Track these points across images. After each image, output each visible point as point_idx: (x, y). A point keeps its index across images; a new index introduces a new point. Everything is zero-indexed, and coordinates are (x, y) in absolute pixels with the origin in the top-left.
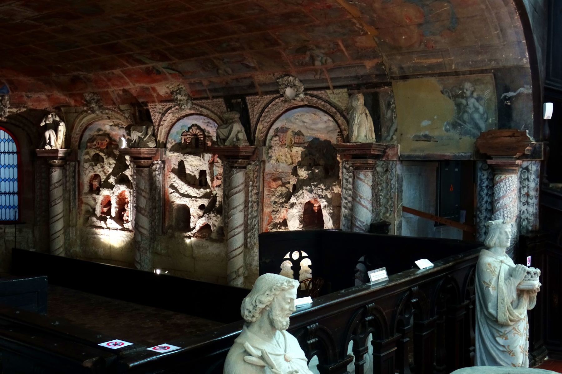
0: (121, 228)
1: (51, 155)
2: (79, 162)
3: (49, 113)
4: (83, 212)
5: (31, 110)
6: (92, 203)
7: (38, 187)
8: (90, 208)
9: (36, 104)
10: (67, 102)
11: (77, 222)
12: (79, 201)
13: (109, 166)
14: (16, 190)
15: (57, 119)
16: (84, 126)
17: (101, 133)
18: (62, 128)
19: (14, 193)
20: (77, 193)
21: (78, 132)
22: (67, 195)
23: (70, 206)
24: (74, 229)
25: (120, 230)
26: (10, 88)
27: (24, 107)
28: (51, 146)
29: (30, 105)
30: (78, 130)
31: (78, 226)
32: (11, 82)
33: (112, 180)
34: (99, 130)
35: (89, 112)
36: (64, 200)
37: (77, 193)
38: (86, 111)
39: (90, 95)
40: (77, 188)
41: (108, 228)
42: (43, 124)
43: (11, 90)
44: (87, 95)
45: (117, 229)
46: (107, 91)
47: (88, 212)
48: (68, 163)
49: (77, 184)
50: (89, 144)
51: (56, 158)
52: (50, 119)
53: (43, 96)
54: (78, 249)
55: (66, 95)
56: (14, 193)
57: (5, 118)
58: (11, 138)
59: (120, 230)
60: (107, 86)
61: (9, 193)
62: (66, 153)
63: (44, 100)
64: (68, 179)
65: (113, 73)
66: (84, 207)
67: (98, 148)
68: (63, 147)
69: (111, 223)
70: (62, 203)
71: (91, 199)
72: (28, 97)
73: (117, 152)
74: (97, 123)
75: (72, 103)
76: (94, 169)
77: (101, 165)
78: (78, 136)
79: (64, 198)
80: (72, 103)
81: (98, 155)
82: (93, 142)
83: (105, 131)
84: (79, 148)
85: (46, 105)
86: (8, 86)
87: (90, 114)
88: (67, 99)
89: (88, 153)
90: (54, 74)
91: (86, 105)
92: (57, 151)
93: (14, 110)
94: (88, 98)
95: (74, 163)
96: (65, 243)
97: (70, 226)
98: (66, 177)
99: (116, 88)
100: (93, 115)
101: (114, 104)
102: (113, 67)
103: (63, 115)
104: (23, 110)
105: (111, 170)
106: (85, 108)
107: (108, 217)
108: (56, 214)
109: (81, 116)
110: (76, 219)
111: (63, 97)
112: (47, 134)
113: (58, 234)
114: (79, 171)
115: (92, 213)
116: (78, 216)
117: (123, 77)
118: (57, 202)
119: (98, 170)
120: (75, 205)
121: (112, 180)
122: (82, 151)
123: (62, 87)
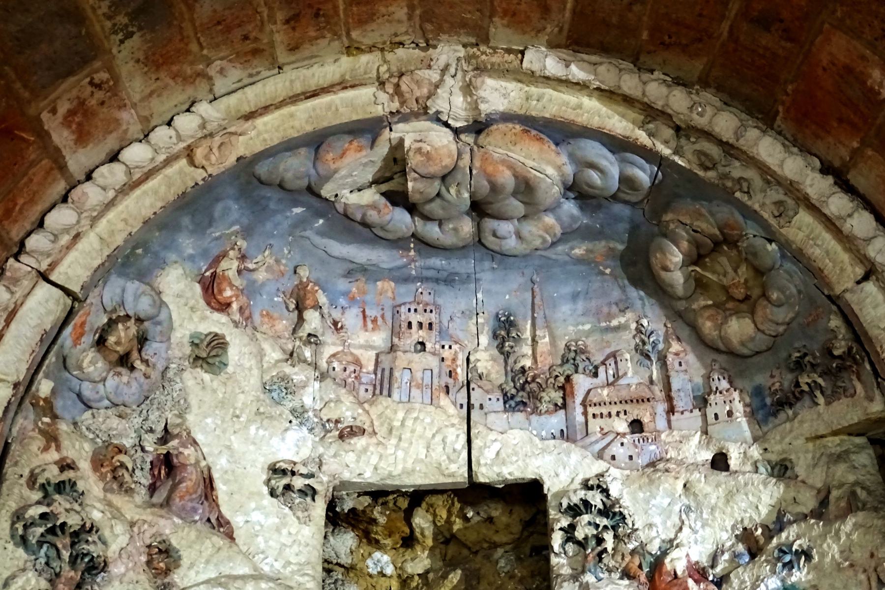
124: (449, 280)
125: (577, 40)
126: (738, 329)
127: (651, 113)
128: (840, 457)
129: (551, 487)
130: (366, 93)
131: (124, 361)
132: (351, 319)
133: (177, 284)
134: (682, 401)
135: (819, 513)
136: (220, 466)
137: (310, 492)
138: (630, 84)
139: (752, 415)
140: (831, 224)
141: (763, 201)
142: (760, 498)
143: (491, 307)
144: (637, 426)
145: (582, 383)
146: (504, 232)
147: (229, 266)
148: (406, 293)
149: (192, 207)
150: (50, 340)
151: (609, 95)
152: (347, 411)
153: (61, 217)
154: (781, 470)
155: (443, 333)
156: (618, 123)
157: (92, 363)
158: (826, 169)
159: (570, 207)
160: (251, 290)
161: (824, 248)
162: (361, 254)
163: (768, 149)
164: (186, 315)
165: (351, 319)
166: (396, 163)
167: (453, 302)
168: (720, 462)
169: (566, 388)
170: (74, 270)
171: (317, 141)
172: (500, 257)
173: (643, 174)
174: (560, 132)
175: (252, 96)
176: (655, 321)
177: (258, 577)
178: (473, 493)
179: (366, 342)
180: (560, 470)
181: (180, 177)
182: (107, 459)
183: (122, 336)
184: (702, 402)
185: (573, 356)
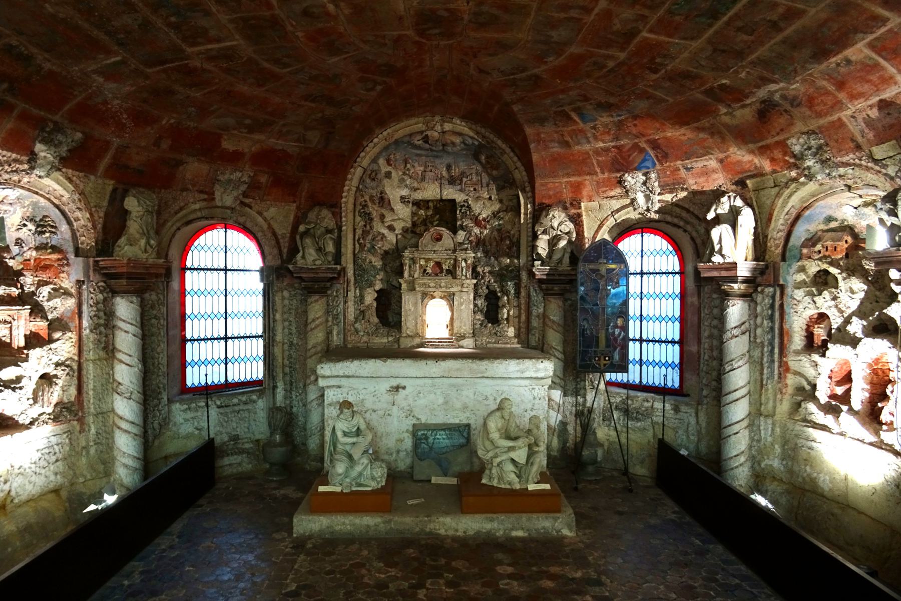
0: (873, 439)
1: (724, 274)
2: (782, 288)
3: (723, 194)
4: (790, 390)
5: (694, 193)
6: (810, 372)
7: (706, 334)
8: (805, 384)
9: (702, 180)
10: (756, 167)
11: (775, 407)
12: (780, 366)
13: (852, 292)
14: (677, 338)
15: (739, 202)
16: (794, 213)
17: (833, 225)
18: (747, 219)
19: (673, 342)
20: (776, 350)
21: (781, 227)
22: (757, 353)
23: (762, 374)
24: (770, 421)
25: (871, 444)
26: (657, 156)
27: (683, 189)
28: (723, 256)
29: (693, 183)
30: (781, 221)
31: (777, 417)
32: (655, 145)
33: (856, 327)
34: (830, 219)
35: (802, 179)
36: (751, 361)
37: (776, 350)
38: (795, 180)
39: (801, 140)
40: (777, 341)
41: (842, 434)
42: (711, 216)
43: (659, 161)
44: (794, 141)
45: (862, 441)
46: (840, 119)
47: (800, 390)
48: (759, 289)
49: (777, 331)
50: (805, 251)
51: (734, 279)
52: (724, 207)
53: (713, 163)
54: (776, 463)
55: (751, 152)
56: (673, 342)
57: (656, 212)
58: (671, 248)
59: (871, 444)
60: (838, 105)
61: (667, 342)
62: (754, 270)
63: (714, 171)
64: (759, 320)
65: (848, 62)
66: (791, 380)
67: (825, 257)
68: (750, 257)
69: (848, 423)
70: (746, 368)
71: (807, 365)
72: (687, 169)
73: (870, 266)
74: (822, 203)
75: (767, 166)
76: (815, 302)
77: (830, 293)
78: (782, 235)
79: (750, 357)
80: (767, 166)
81: (826, 272)
82: (814, 245)
83: (844, 221)
84: (784, 259)
85: (719, 180)
86: (651, 153)
87: (804, 184)
88: (756, 161)
89: (802, 269)
90: (723, 110)
91: (795, 166)
92: (733, 266)
93: (668, 197)
94: (797, 149)
95: (771, 289)
96: (750, 447)
97: (761, 415)
98: (756, 317)
99: (860, 104)
100: (812, 187)
101: (858, 147)
102: (843, 41)
103: (752, 194)
104: (682, 195)
105: (854, 305)
106: (793, 174)
107: (845, 408)
108: (733, 388)
109: (787, 192)
110: (775, 401)
111: (747, 158)
112: (715, 233)
113: (736, 428)
114: (782, 306)
115: (808, 392)
116: (779, 396)
117: (876, 66)
118: (736, 366)
119: (824, 303)
120: (772, 372)
121: (856, 327)
122: (790, 265)
123: (743, 136)
124: (437, 157)
125: (463, 118)
126: (495, 173)
127: (477, 133)
128: (511, 200)
129: (458, 201)
130: (421, 125)
131: (373, 179)
132: (416, 164)
133: (382, 161)
134: (484, 185)
135: (505, 211)
136: (391, 197)
137: (409, 202)
138: (474, 127)
139: (497, 190)
140: (511, 158)
141: (498, 152)
142: (497, 207)
143: (446, 162)
144: (475, 190)
145: (465, 180)
146: (449, 149)
147: (392, 156)
148: (428, 159)
149: (386, 148)
150: (361, 178)
151: (470, 128)
152: (416, 185)
153: (363, 154)
154: (501, 201)
155: (436, 168)
156: (471, 134)
157: (368, 181)
158: (510, 147)
159: (462, 145)
160: (396, 160)
161: (509, 163)
162: (419, 152)
163: (499, 142)
164: (385, 168)
165: (416, 164)
166: (427, 136)
167: (438, 161)
168: (490, 198)
169: (461, 180)
170: (365, 163)
171: (411, 135)
172: (448, 153)
173: (476, 143)
174: (460, 134)
175: (398, 126)
176: (479, 168)
177: (399, 219)
178: (441, 200)
179: (420, 169)
180: (460, 197)
181: (384, 143)
182: (372, 198)
183: (374, 174)
184: (488, 186)
185: (463, 174)
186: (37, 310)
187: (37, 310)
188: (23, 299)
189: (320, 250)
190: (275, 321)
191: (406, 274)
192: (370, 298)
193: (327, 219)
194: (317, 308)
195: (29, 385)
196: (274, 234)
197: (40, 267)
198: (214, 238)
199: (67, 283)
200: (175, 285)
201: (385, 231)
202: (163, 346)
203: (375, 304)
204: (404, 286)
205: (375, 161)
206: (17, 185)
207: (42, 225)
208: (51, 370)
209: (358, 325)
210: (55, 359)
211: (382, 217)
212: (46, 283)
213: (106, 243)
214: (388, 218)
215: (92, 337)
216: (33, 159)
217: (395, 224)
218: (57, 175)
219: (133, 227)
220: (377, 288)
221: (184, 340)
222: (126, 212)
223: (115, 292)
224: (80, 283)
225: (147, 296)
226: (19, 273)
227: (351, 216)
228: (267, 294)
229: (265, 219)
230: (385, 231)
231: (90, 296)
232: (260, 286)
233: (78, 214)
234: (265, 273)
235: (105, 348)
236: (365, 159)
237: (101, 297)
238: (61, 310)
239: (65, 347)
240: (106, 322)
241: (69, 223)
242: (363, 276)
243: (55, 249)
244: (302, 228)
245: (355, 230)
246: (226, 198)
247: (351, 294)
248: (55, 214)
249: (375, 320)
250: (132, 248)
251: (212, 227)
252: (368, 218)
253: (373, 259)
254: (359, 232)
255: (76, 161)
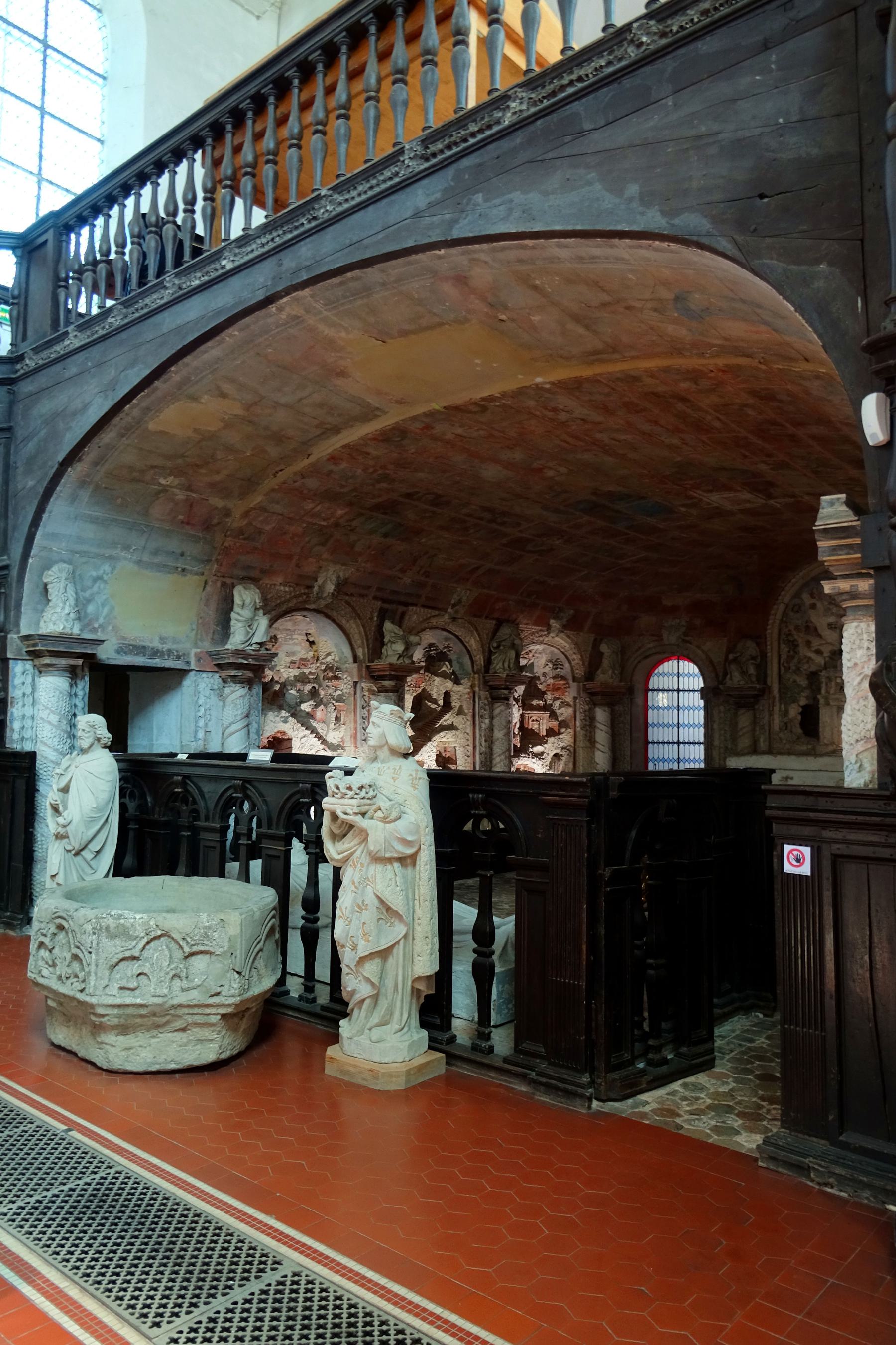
133: (806, 597)
136: (818, 625)
157: (792, 614)
170: (787, 600)
182: (797, 628)
186: (553, 715)
187: (553, 715)
188: (546, 708)
189: (744, 673)
190: (712, 729)
191: (823, 691)
192: (794, 712)
193: (751, 648)
194: (744, 720)
195: (548, 759)
196: (711, 662)
197: (556, 689)
198: (670, 666)
199: (569, 699)
200: (639, 701)
201: (813, 655)
202: (628, 743)
203: (799, 718)
204: (822, 701)
205: (798, 595)
206: (542, 643)
207: (556, 664)
208: (558, 751)
209: (781, 735)
210: (562, 744)
211: (808, 643)
212: (558, 699)
213: (590, 676)
214: (816, 643)
215: (582, 732)
216: (549, 628)
217: (822, 648)
218: (562, 635)
219: (606, 662)
220: (803, 702)
221: (647, 743)
222: (602, 653)
223: (595, 705)
224: (575, 698)
225: (616, 708)
226: (544, 693)
227: (775, 644)
228: (706, 708)
229: (703, 651)
230: (813, 655)
231: (581, 707)
232: (702, 703)
233: (575, 656)
234: (704, 693)
235: (590, 740)
236: (786, 596)
237: (587, 707)
238: (566, 715)
239: (566, 738)
240: (590, 724)
241: (570, 662)
242: (787, 694)
243: (563, 678)
244: (731, 656)
245: (779, 656)
246: (671, 638)
247: (776, 709)
248: (562, 657)
249: (800, 731)
250: (605, 676)
251: (668, 659)
252: (794, 645)
253: (798, 679)
254: (784, 657)
255: (572, 626)
